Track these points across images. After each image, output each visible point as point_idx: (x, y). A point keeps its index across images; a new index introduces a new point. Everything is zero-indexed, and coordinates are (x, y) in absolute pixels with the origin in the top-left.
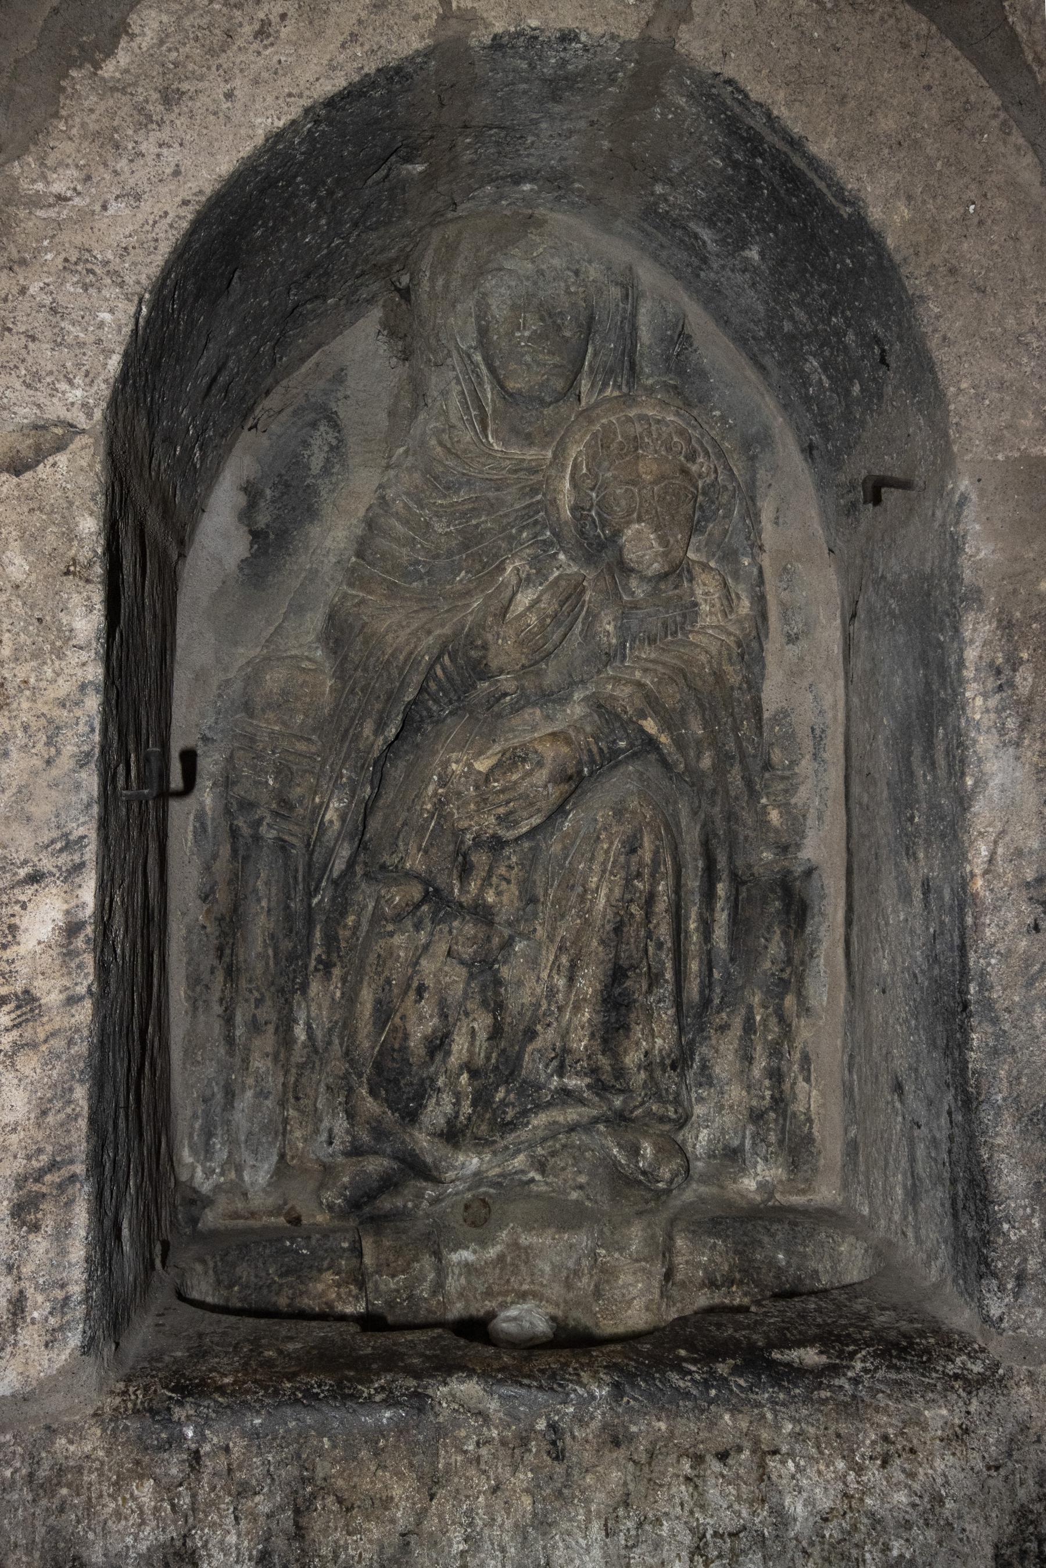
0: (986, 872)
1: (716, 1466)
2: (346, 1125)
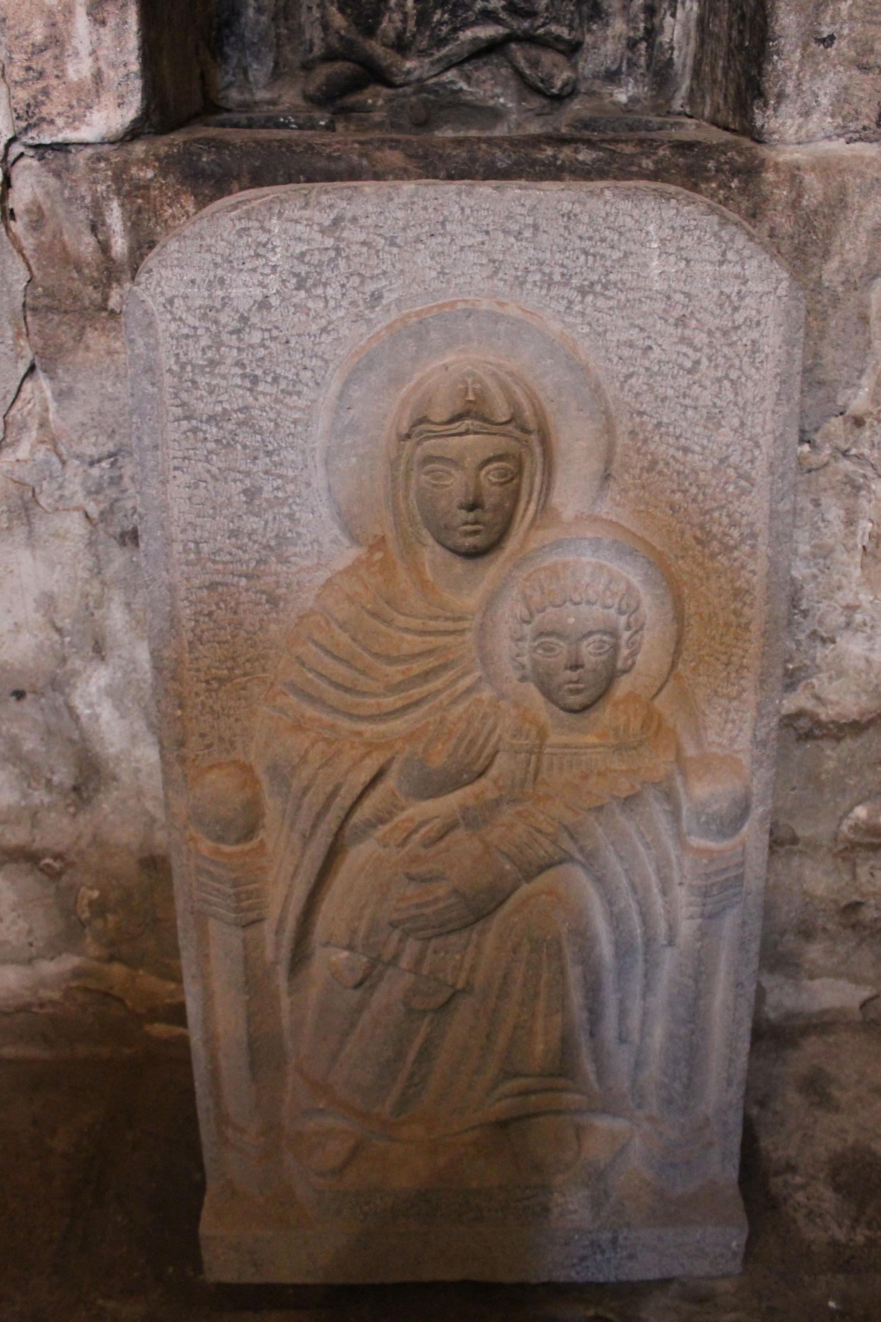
2: (322, 35)
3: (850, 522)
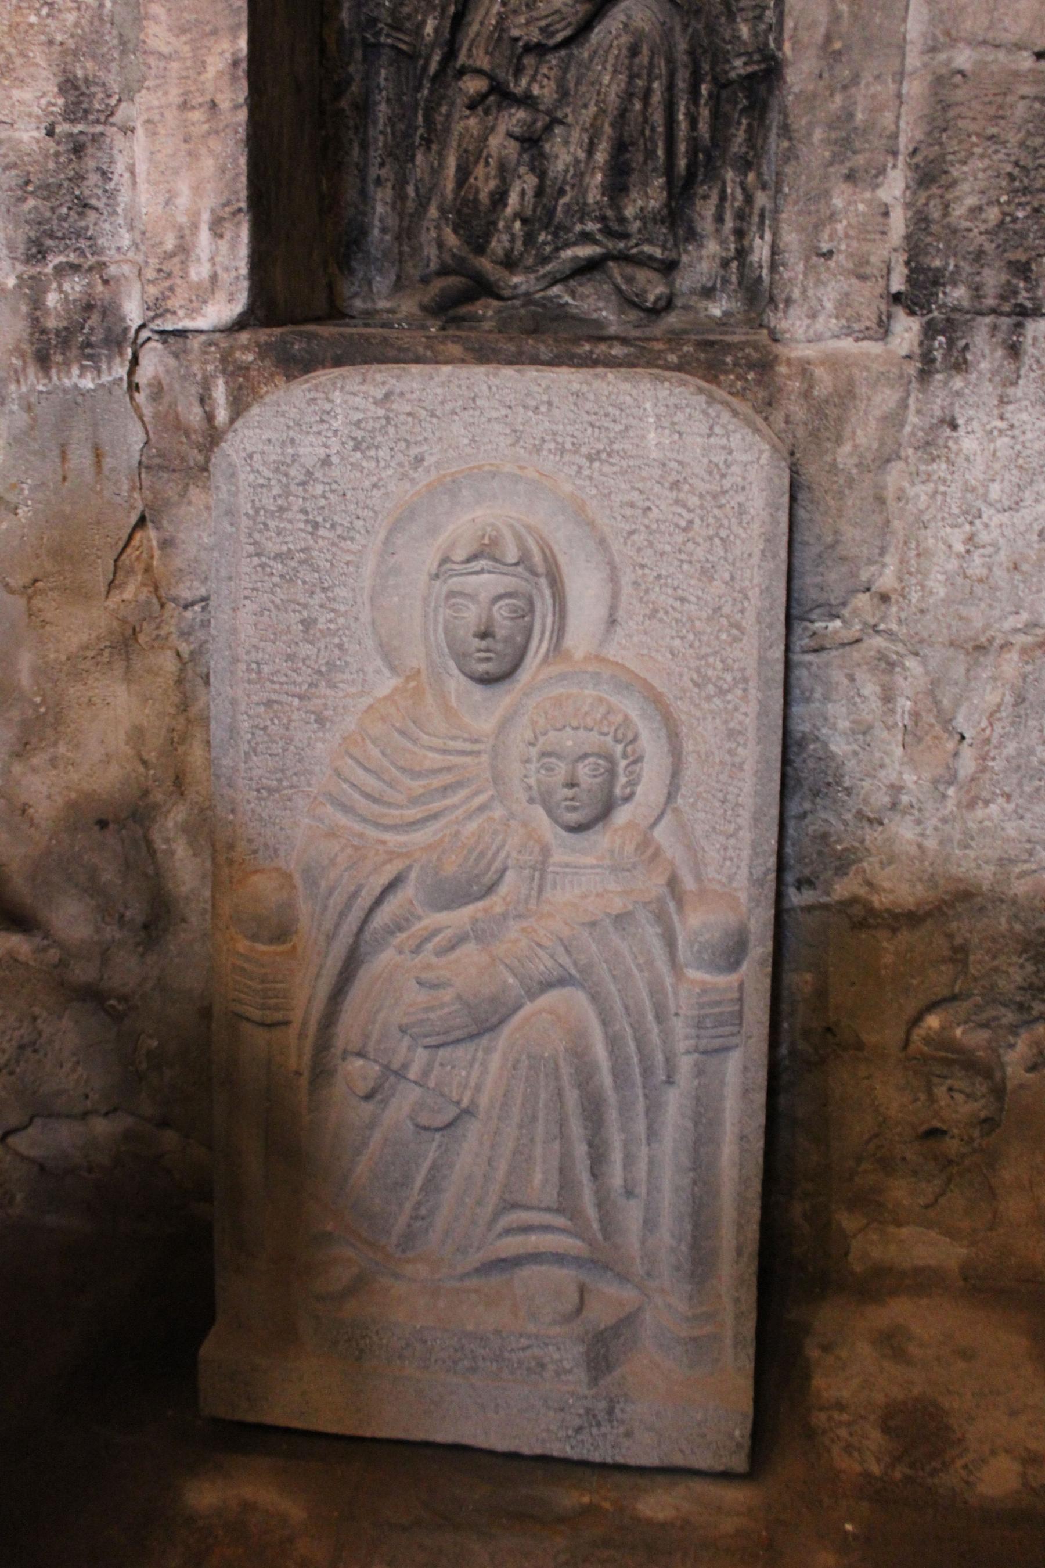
3: (888, 697)
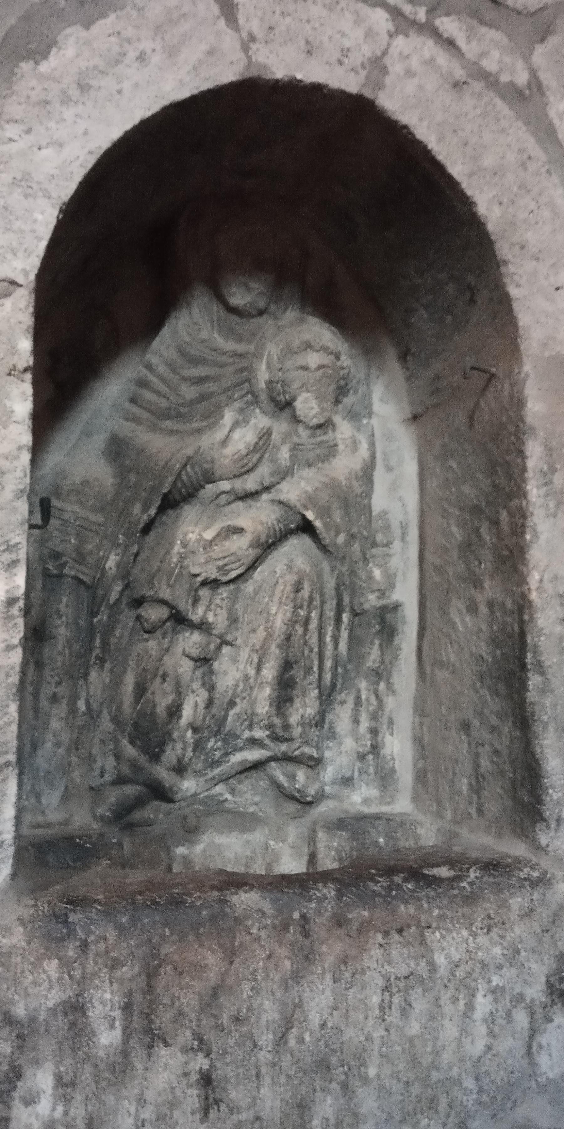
0: (538, 588)
1: (396, 936)
